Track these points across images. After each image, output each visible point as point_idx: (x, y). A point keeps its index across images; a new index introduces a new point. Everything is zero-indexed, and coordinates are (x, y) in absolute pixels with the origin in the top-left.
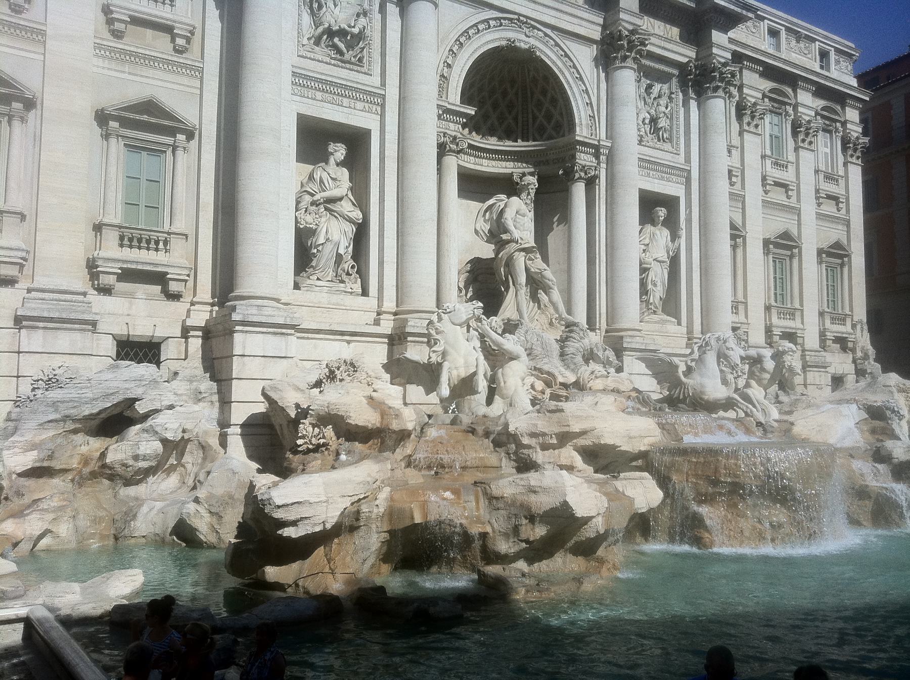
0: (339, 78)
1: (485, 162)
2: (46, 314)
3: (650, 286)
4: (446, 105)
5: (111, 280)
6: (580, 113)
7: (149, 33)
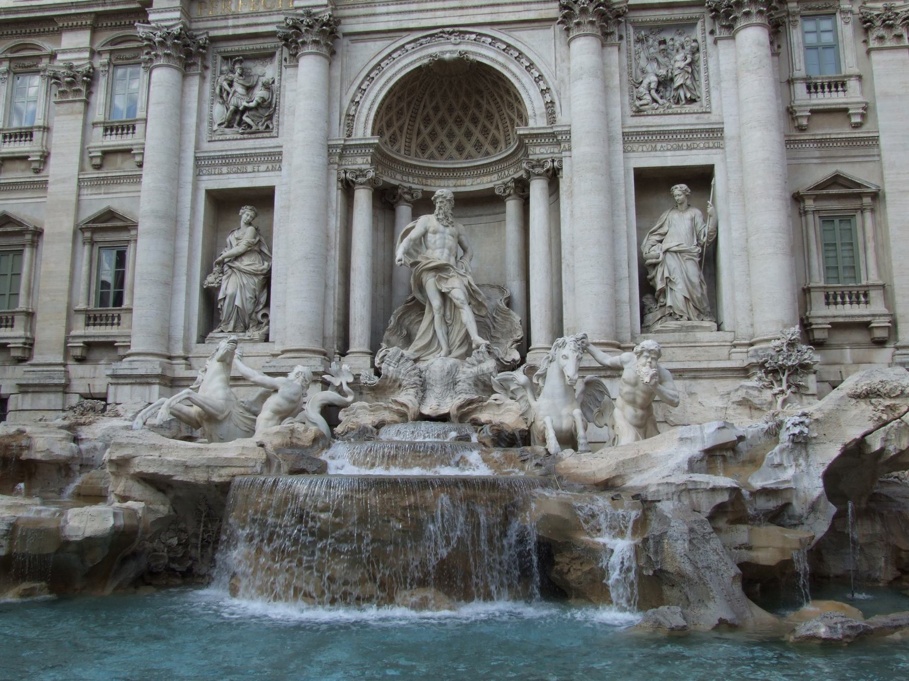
0: (238, 150)
1: (468, 182)
2: (31, 382)
3: (659, 286)
4: (342, 142)
5: (78, 352)
6: (533, 102)
7: (119, 159)
